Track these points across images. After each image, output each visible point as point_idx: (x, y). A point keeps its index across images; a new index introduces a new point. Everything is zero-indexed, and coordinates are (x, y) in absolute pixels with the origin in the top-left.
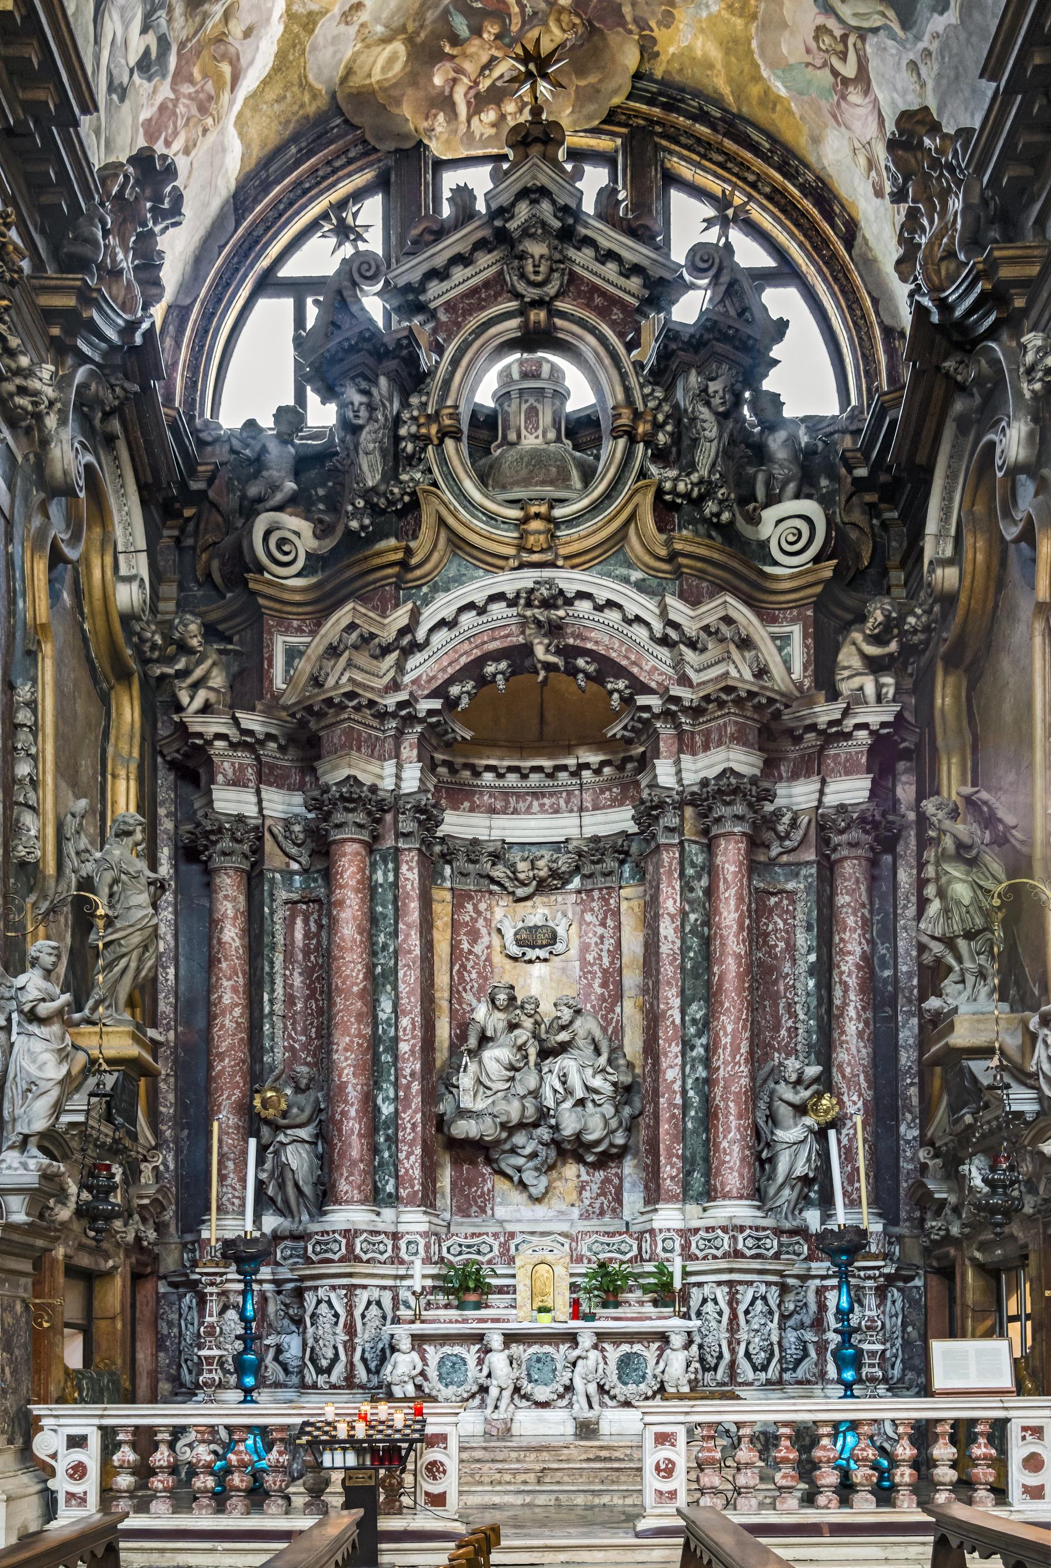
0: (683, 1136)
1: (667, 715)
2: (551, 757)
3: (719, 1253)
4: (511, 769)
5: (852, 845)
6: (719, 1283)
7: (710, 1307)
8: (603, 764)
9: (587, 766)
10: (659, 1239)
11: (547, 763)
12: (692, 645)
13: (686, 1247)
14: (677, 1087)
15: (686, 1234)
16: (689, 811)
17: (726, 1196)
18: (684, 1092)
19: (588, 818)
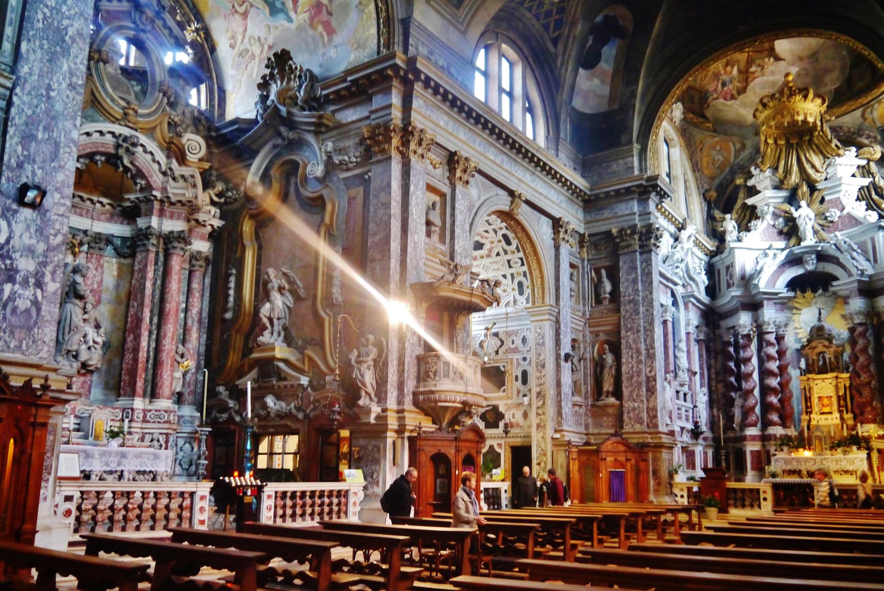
0: (146, 370)
1: (162, 202)
2: (87, 194)
3: (162, 421)
4: (88, 199)
5: (201, 266)
6: (161, 434)
7: (155, 443)
8: (109, 204)
9: (101, 203)
10: (136, 412)
11: (85, 196)
12: (174, 179)
13: (145, 416)
14: (146, 349)
15: (145, 411)
16: (162, 240)
17: (163, 398)
18: (148, 352)
19: (96, 223)
